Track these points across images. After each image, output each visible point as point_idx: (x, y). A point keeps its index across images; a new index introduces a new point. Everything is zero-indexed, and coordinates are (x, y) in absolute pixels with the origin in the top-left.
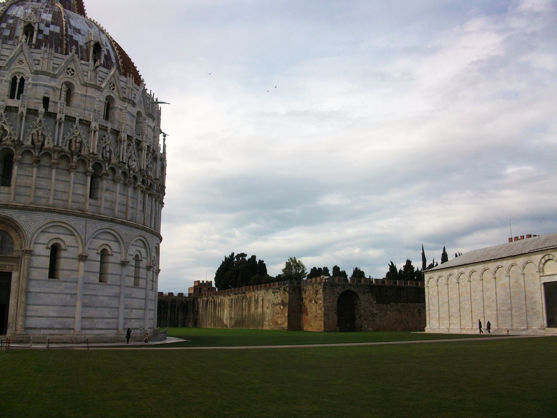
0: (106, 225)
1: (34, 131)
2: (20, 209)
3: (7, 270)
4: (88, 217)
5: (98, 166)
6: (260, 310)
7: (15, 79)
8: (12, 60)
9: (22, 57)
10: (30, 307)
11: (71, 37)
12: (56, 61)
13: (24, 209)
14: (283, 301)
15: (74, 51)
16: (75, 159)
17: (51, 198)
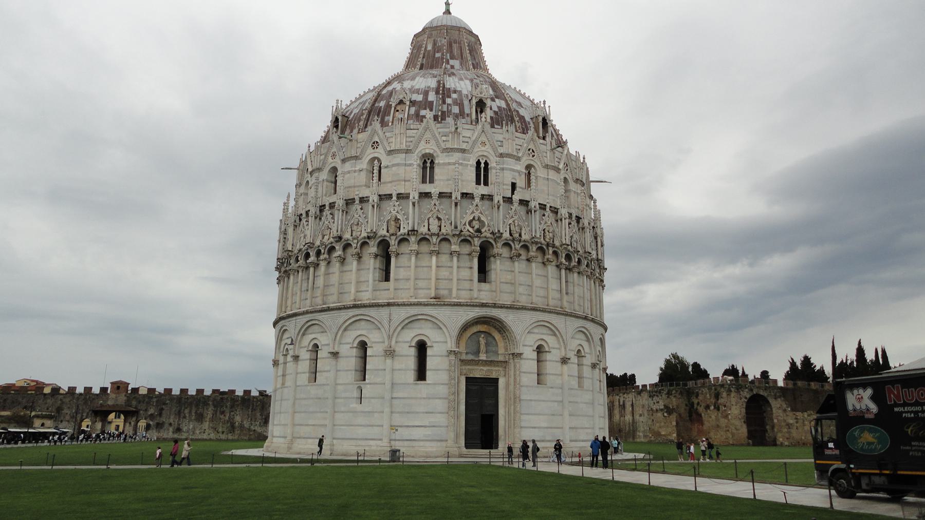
0: (581, 323)
1: (511, 221)
2: (507, 308)
3: (494, 376)
4: (567, 314)
5: (568, 257)
6: (628, 418)
7: (478, 163)
8: (475, 142)
9: (483, 138)
10: (523, 417)
11: (518, 112)
12: (520, 142)
13: (510, 307)
14: (666, 407)
15: (532, 129)
16: (551, 250)
17: (534, 295)
